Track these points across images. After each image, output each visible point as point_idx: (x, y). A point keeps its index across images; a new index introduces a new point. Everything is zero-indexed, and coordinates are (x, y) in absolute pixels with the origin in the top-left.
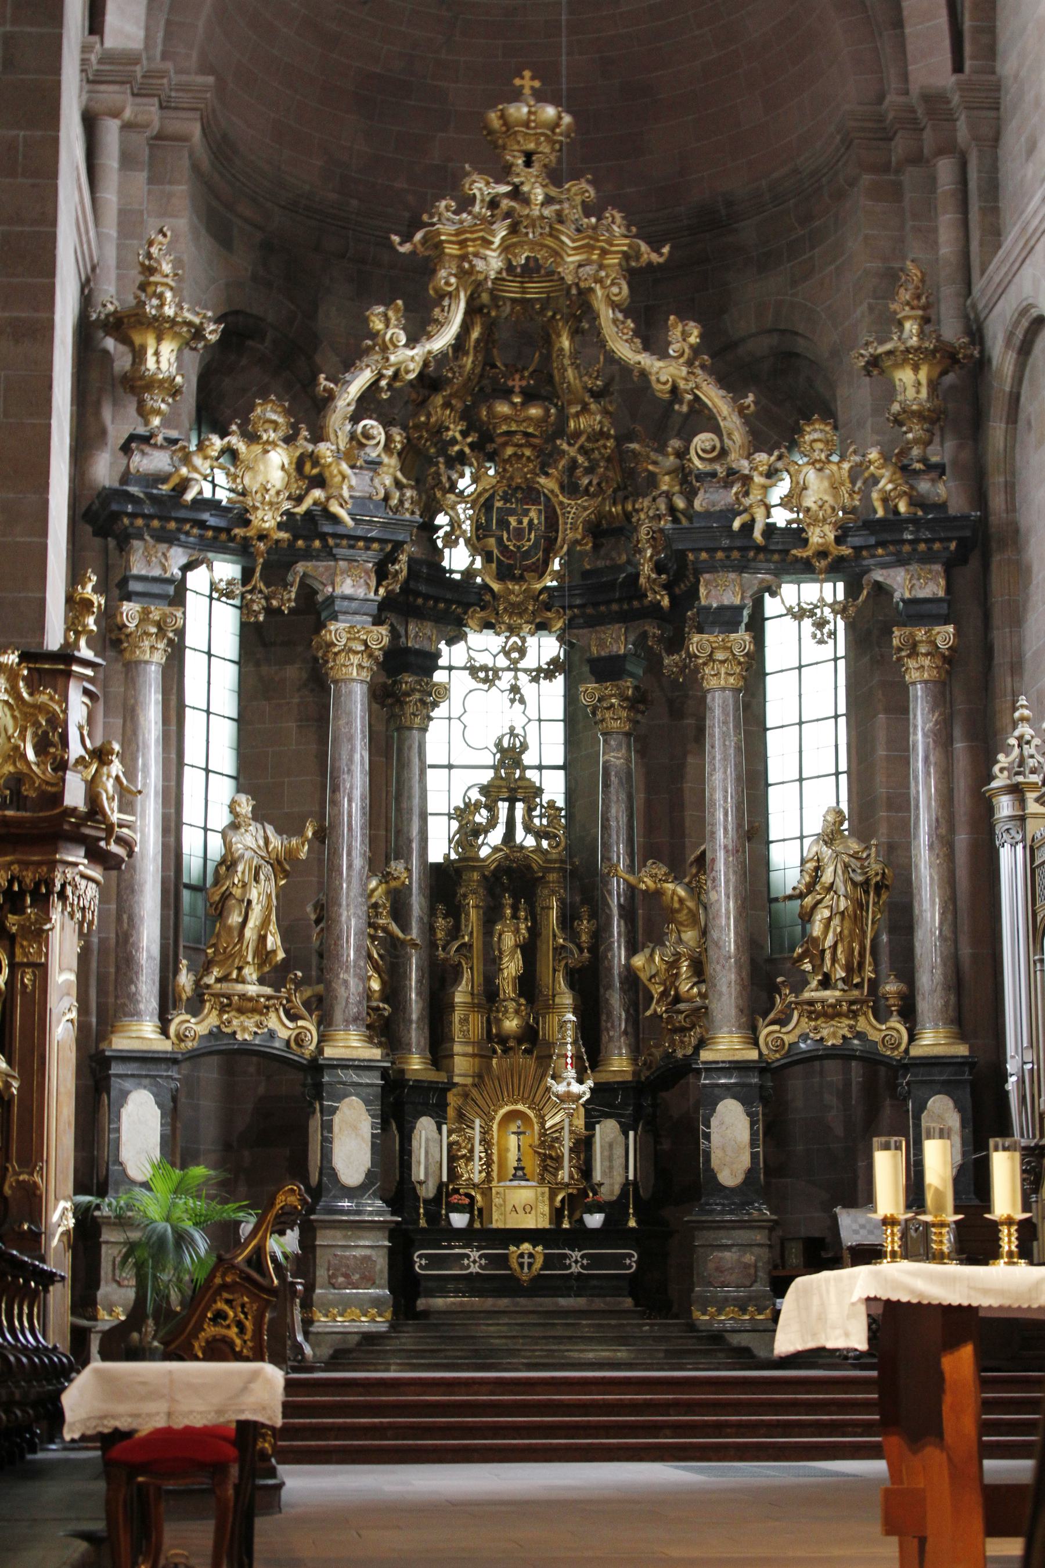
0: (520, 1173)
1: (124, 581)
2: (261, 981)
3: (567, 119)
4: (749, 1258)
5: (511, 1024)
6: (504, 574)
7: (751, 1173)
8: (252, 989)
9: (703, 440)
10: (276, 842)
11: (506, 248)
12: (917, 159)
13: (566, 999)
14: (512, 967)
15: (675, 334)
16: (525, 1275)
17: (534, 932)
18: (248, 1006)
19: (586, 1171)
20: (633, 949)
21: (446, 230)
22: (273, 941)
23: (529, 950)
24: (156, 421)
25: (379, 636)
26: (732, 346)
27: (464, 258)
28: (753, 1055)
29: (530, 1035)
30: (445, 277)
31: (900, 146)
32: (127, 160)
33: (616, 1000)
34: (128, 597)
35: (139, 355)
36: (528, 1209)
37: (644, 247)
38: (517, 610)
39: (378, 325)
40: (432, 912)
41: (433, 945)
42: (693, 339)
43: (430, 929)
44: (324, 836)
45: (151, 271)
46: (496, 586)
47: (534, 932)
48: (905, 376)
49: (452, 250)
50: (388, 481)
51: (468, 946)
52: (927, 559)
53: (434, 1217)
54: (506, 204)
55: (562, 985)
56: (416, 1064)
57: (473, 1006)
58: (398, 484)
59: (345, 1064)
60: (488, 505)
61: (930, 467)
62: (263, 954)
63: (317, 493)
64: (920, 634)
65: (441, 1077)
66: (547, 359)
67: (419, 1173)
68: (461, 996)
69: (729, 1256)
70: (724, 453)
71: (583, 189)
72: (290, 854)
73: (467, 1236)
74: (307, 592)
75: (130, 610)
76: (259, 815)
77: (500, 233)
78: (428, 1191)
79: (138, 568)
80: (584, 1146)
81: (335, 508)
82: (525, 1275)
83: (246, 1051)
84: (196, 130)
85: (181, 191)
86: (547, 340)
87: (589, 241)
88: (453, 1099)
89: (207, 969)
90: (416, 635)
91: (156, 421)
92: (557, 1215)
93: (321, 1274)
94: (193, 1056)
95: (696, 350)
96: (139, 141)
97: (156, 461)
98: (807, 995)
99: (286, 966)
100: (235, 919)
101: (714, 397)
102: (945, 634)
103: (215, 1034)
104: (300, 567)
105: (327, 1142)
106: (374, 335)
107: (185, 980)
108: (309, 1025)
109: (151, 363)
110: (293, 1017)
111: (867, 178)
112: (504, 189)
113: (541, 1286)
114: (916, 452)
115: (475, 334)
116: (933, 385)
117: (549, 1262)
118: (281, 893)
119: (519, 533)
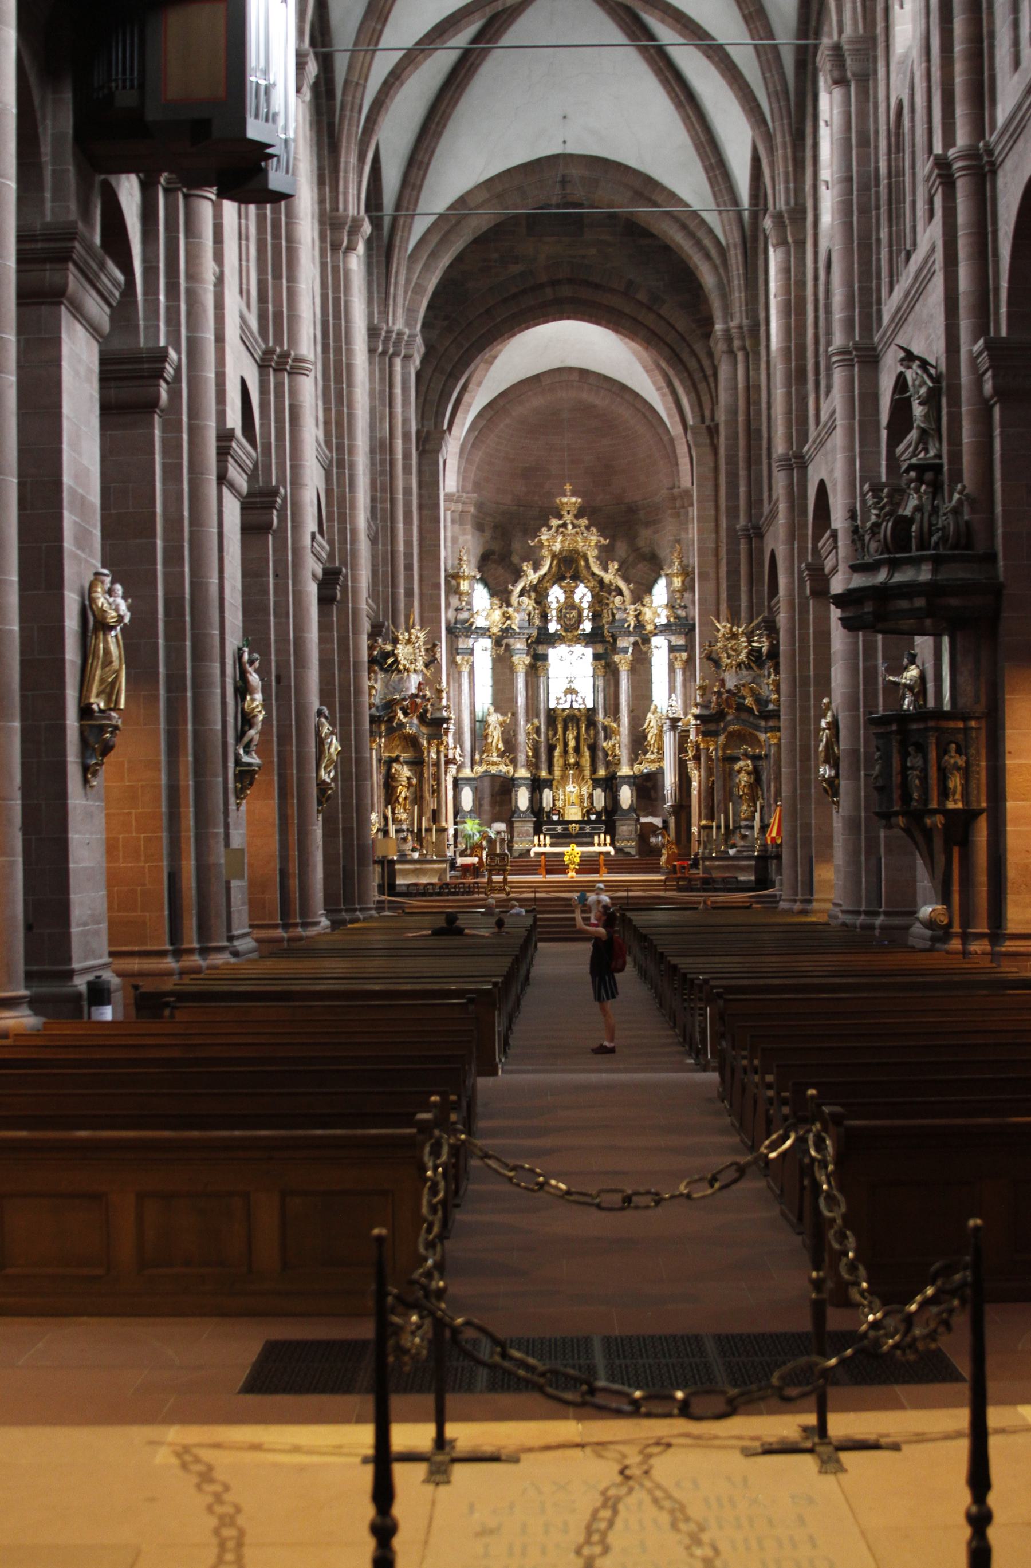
0: (573, 804)
1: (457, 649)
2: (498, 756)
3: (579, 500)
4: (630, 828)
5: (572, 761)
6: (566, 631)
7: (631, 806)
8: (495, 759)
9: (619, 598)
10: (501, 718)
11: (562, 542)
12: (683, 507)
13: (587, 753)
14: (572, 744)
15: (610, 566)
16: (574, 833)
17: (578, 733)
18: (494, 764)
19: (592, 804)
20: (606, 738)
21: (544, 538)
22: (501, 746)
23: (577, 739)
24: (464, 603)
25: (527, 660)
26: (639, 549)
27: (549, 546)
28: (631, 773)
29: (577, 765)
30: (545, 552)
31: (678, 504)
32: (453, 522)
33: (600, 754)
34: (458, 654)
35: (458, 584)
36: (575, 814)
37: (602, 539)
38: (571, 640)
39: (525, 568)
40: (547, 730)
41: (548, 740)
42: (616, 567)
43: (547, 735)
44: (514, 714)
45: (461, 560)
46: (564, 634)
47: (578, 733)
48: (675, 580)
49: (546, 543)
50: (530, 608)
51: (558, 739)
52: (680, 633)
53: (549, 817)
54: (561, 530)
55: (586, 749)
56: (544, 774)
57: (560, 756)
58: (534, 609)
59: (520, 778)
60: (561, 611)
61: (681, 607)
62: (498, 749)
63: (509, 622)
64: (678, 655)
65: (551, 777)
66: (577, 567)
67: (544, 805)
68: (557, 753)
69: (625, 828)
70: (624, 601)
71: (584, 522)
72: (504, 721)
73: (558, 823)
74: (508, 645)
75: (459, 658)
76: (496, 711)
77: (560, 538)
78: (547, 809)
79: (460, 646)
80: (591, 796)
81: (513, 626)
82: (574, 833)
83: (494, 776)
84: (472, 509)
85: (469, 527)
86: (577, 561)
87: (585, 539)
88: (555, 783)
89: (484, 752)
90: (541, 649)
91: (464, 603)
92: (583, 815)
93: (515, 834)
94: (480, 777)
95: (618, 570)
96: (457, 515)
97: (464, 615)
98: (647, 756)
99: (504, 752)
100: (490, 740)
101: (622, 585)
102: (685, 655)
103: (486, 771)
104: (505, 641)
105: (516, 799)
106: (524, 571)
107: (477, 757)
108: (511, 768)
109: (462, 587)
110: (507, 766)
111: (670, 511)
112: (561, 522)
113: (578, 836)
114: (678, 601)
115: (555, 562)
116: (683, 582)
117: (580, 829)
118: (503, 733)
119: (570, 619)
